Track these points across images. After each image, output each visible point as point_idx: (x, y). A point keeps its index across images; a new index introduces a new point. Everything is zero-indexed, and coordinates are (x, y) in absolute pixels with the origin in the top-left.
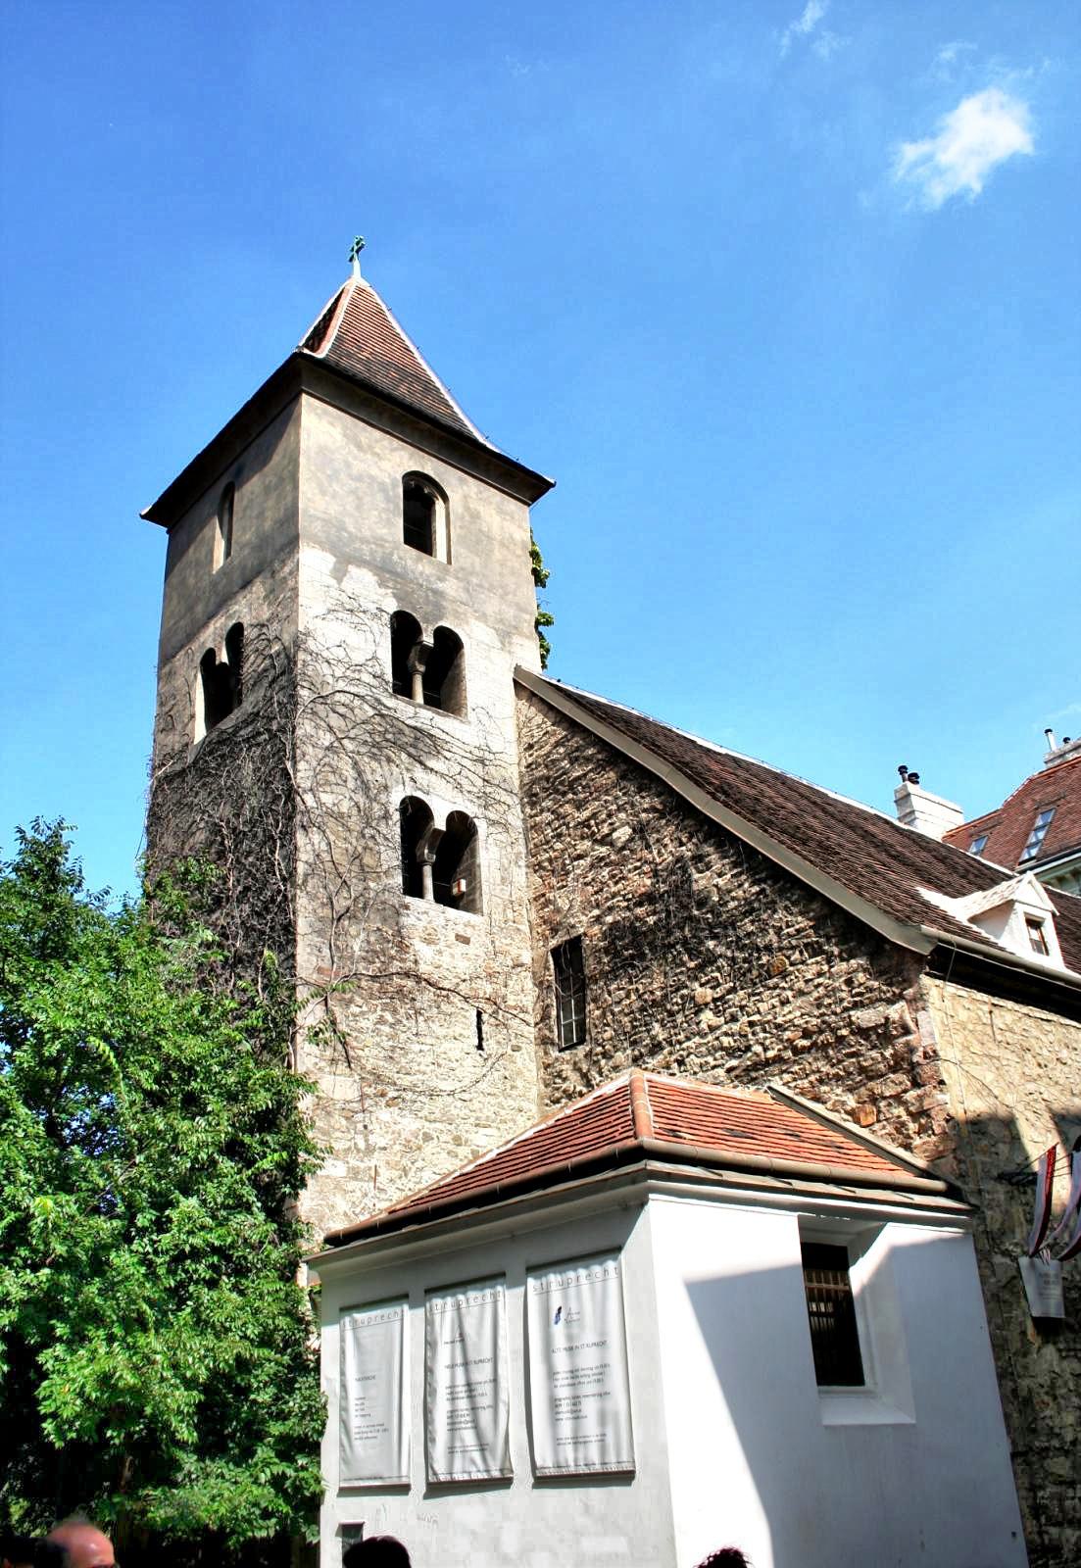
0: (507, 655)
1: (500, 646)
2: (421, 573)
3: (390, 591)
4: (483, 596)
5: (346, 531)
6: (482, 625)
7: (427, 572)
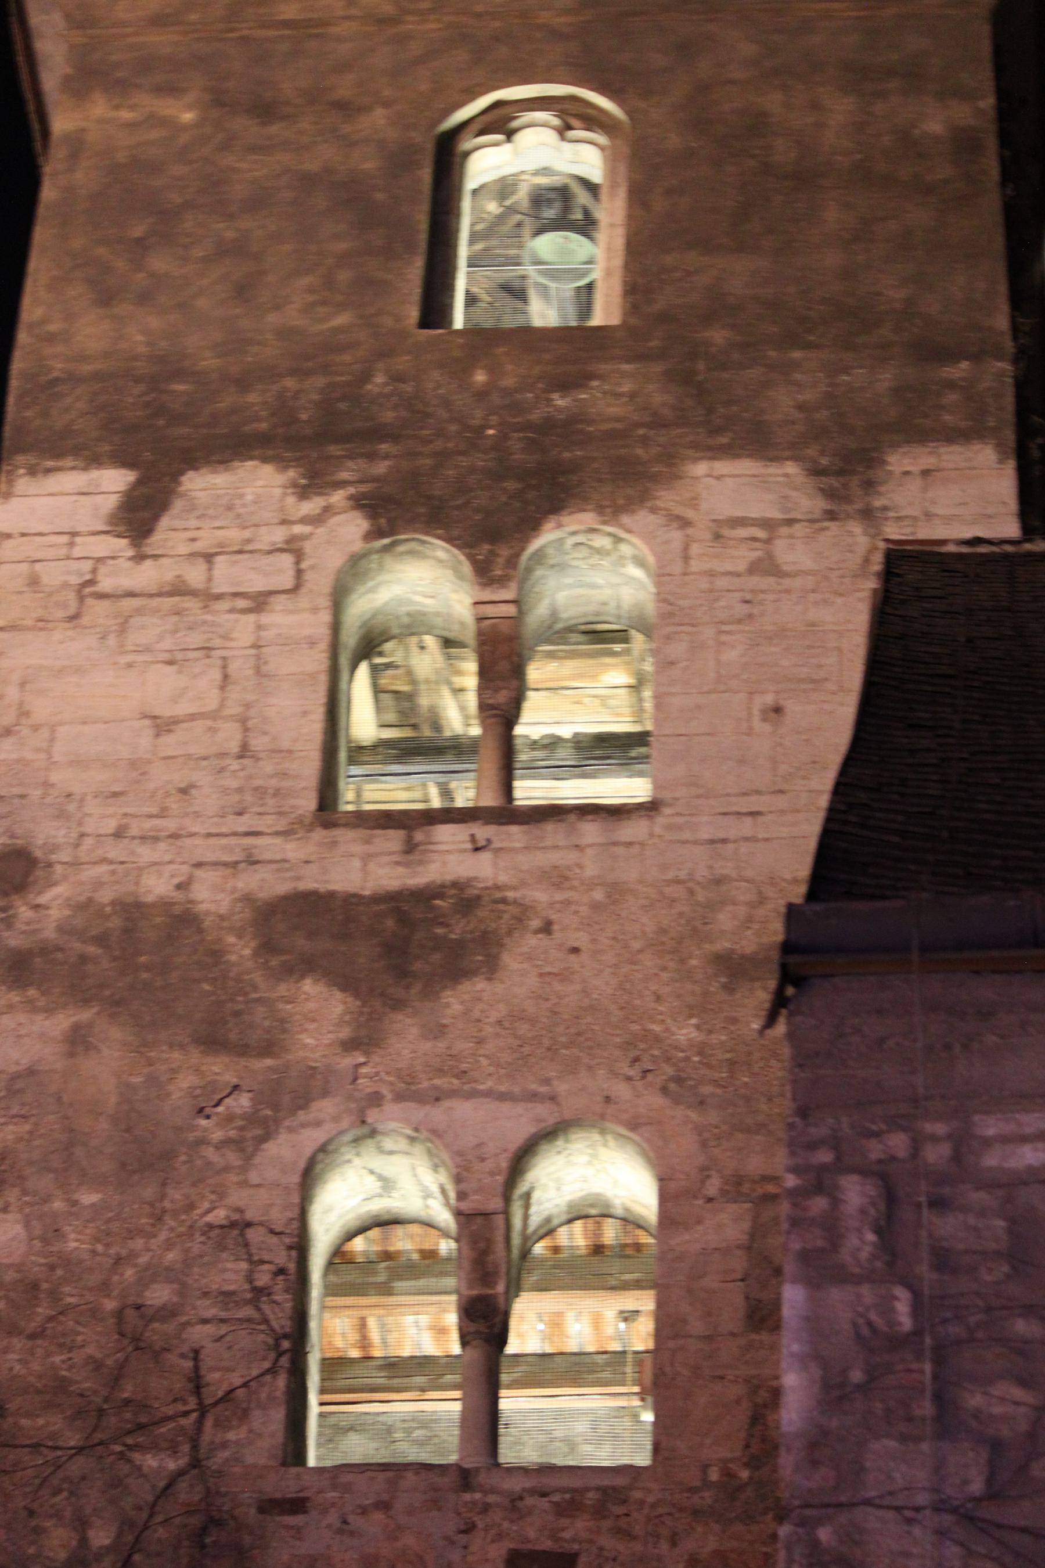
0: (856, 528)
1: (820, 504)
2: (482, 395)
3: (338, 497)
4: (755, 373)
5: (178, 374)
6: (746, 466)
7: (509, 382)
